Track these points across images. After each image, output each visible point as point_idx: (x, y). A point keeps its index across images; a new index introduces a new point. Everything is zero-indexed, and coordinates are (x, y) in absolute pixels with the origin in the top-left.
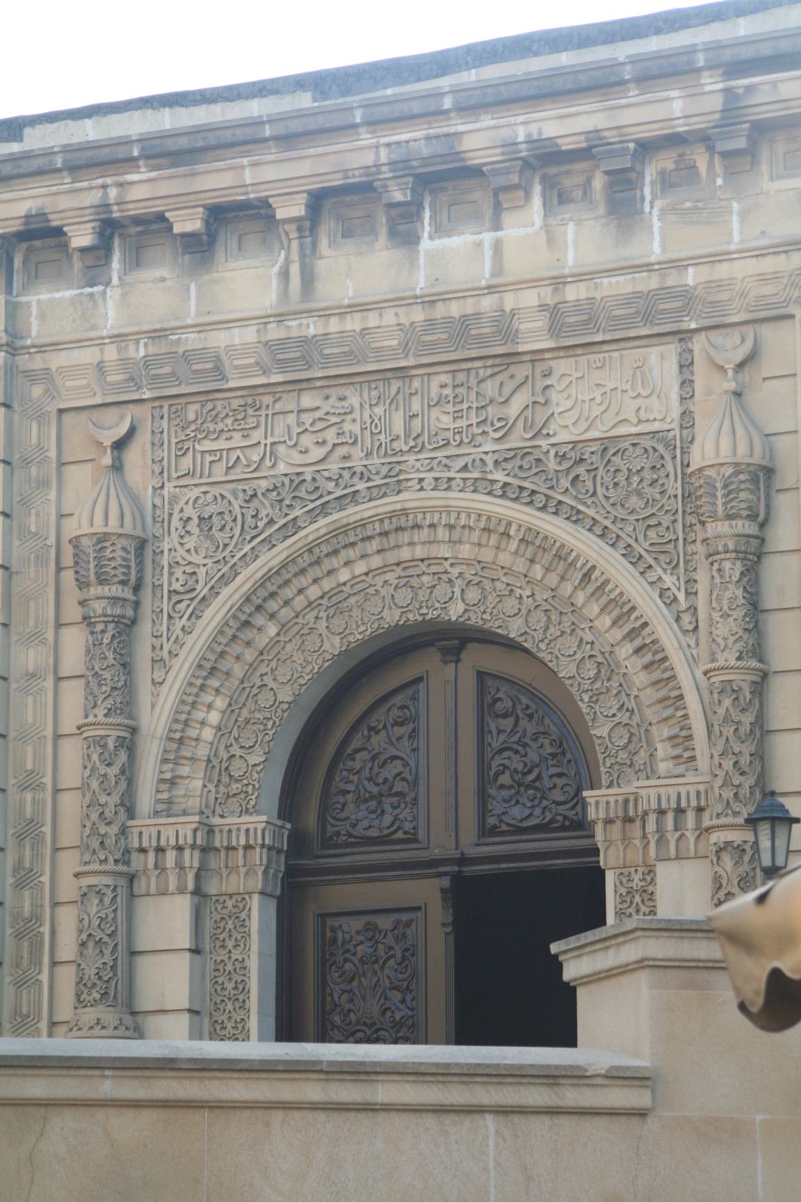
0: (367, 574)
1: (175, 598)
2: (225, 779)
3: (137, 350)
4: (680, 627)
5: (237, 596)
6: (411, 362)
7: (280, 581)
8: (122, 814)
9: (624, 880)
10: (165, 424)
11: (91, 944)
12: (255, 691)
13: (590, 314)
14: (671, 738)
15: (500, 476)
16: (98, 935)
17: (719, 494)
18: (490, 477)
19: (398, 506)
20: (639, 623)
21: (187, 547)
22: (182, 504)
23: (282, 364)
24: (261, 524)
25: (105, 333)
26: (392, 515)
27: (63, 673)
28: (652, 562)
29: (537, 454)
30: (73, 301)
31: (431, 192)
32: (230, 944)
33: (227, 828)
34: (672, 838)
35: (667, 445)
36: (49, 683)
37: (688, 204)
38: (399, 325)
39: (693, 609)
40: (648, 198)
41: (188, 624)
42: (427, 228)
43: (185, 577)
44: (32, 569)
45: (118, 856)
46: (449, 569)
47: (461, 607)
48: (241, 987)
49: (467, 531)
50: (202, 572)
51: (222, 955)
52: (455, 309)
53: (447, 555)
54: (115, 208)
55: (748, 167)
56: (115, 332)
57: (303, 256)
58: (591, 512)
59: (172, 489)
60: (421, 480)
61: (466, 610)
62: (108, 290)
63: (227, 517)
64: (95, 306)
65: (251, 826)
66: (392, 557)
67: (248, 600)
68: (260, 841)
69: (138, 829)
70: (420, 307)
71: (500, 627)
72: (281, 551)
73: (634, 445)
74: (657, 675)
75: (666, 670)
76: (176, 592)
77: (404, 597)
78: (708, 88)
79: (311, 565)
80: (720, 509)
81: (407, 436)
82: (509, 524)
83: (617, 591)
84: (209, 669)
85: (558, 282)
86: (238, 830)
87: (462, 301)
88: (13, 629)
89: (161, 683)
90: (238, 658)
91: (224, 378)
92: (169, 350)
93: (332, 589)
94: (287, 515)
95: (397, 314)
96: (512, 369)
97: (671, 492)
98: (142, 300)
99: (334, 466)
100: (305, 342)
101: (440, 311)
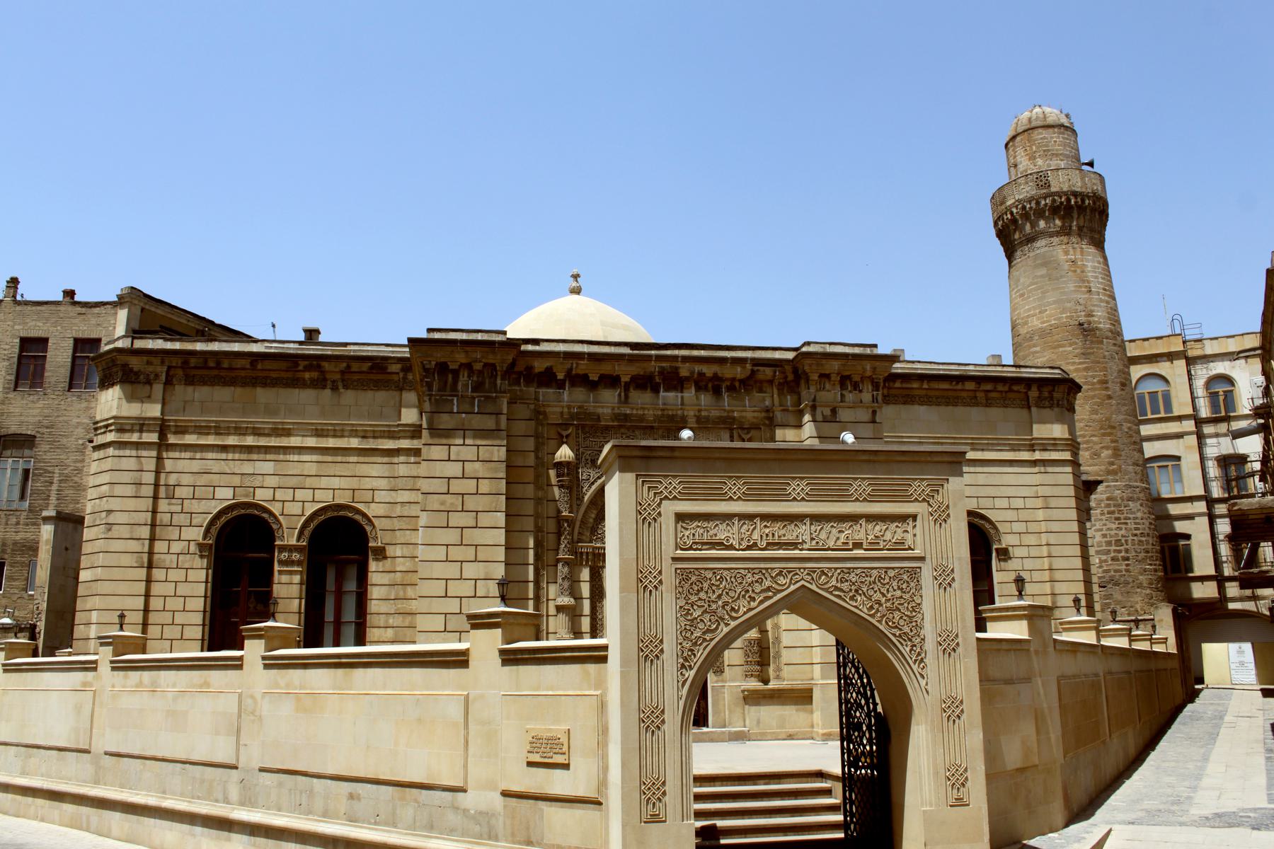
13: (707, 418)
100: (626, 415)
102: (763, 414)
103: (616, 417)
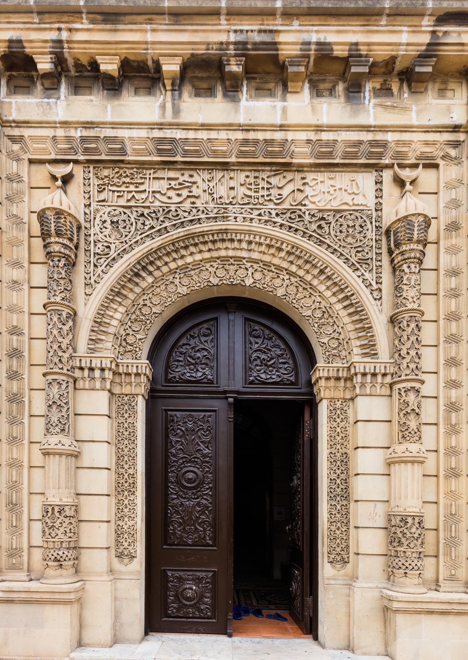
6: (233, 159)
15: (278, 220)
18: (273, 220)
19: (224, 227)
22: (101, 213)
24: (146, 228)
26: (220, 232)
31: (247, 79)
38: (228, 139)
42: (245, 96)
46: (245, 263)
47: (251, 281)
49: (257, 246)
61: (254, 282)
66: (215, 254)
70: (241, 132)
93: (183, 265)
94: (161, 225)
95: (227, 134)
99: (187, 205)
101: (251, 135)
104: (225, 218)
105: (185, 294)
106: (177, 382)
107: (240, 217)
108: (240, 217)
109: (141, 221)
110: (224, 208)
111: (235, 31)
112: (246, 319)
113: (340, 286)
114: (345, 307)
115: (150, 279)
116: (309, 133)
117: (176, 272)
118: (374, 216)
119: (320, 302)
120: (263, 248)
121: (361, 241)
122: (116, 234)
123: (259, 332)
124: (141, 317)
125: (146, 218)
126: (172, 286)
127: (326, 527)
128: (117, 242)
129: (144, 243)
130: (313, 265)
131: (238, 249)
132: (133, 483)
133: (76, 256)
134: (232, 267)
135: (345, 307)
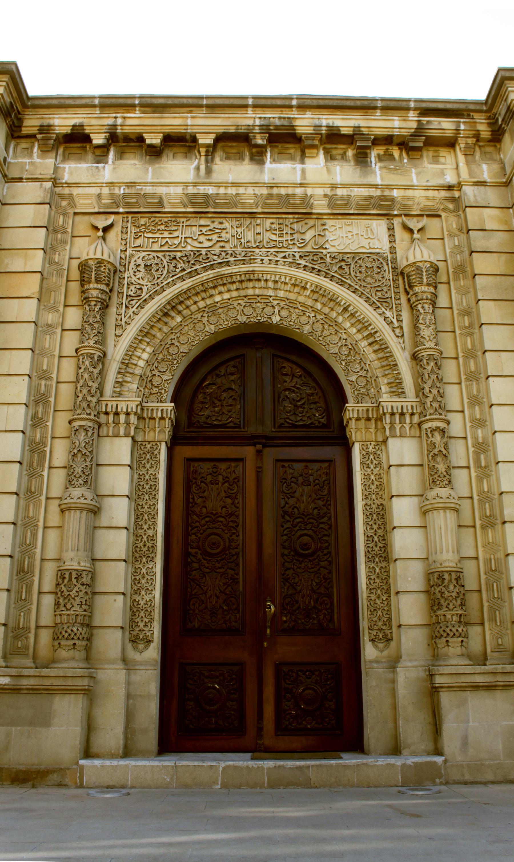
0: (229, 299)
1: (130, 299)
2: (149, 385)
3: (120, 190)
4: (395, 334)
5: (164, 300)
6: (259, 210)
7: (185, 297)
8: (98, 394)
9: (365, 448)
10: (129, 224)
11: (79, 455)
12: (167, 346)
13: (347, 200)
14: (388, 384)
15: (302, 262)
16: (84, 451)
17: (424, 274)
18: (297, 262)
19: (251, 269)
20: (373, 331)
21: (137, 277)
23: (193, 204)
24: (178, 270)
25: (104, 181)
27: (67, 326)
28: (380, 306)
29: (321, 255)
30: (87, 169)
32: (148, 466)
33: (151, 408)
34: (398, 427)
35: (384, 259)
36: (59, 330)
37: (392, 167)
39: (402, 328)
40: (374, 162)
41: (136, 310)
43: (136, 290)
44: (54, 278)
45: (96, 413)
47: (278, 318)
48: (153, 488)
49: (283, 285)
50: (145, 289)
51: (143, 471)
52: (283, 191)
53: (272, 295)
54: (119, 128)
55: (419, 157)
56: (110, 181)
57: (207, 162)
58: (349, 281)
59: (131, 252)
60: (262, 260)
62: (107, 166)
63: (160, 265)
64: (99, 171)
65: (165, 408)
66: (243, 293)
67: (169, 303)
68: (169, 416)
69: (105, 402)
70: (265, 188)
71: (298, 329)
72: (188, 283)
73: (368, 257)
74: (381, 355)
75: (388, 352)
76: (130, 296)
77: (248, 311)
78: (410, 119)
79: (202, 291)
80: (425, 280)
81: (255, 242)
82: (306, 283)
83: (362, 316)
84: (145, 333)
85: (334, 187)
86: (157, 410)
87: (286, 188)
88: (42, 303)
89: (120, 336)
90: (160, 329)
91: (163, 207)
92: (136, 192)
94: (191, 267)
95: (254, 190)
96: (307, 221)
97: (387, 277)
98: (124, 171)
100: (206, 196)
101: (275, 191)
102: (443, 194)
103: (192, 199)
104: (251, 261)
105: (212, 332)
106: (202, 427)
107: (266, 259)
108: (266, 259)
109: (173, 265)
110: (251, 252)
111: (260, 118)
112: (274, 355)
113: (363, 324)
114: (370, 344)
115: (179, 319)
116: (326, 189)
117: (204, 311)
118: (389, 259)
119: (346, 339)
120: (289, 287)
121: (379, 281)
122: (149, 276)
123: (287, 370)
124: (168, 357)
125: (178, 261)
126: (200, 324)
127: (365, 596)
128: (149, 284)
129: (175, 284)
130: (337, 303)
131: (264, 288)
132: (152, 547)
133: (110, 299)
134: (258, 304)
135: (370, 344)
